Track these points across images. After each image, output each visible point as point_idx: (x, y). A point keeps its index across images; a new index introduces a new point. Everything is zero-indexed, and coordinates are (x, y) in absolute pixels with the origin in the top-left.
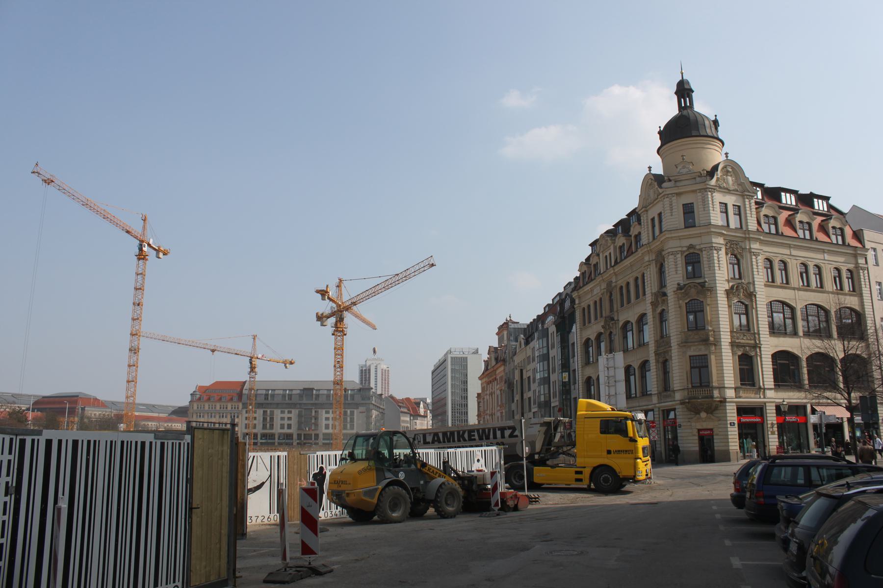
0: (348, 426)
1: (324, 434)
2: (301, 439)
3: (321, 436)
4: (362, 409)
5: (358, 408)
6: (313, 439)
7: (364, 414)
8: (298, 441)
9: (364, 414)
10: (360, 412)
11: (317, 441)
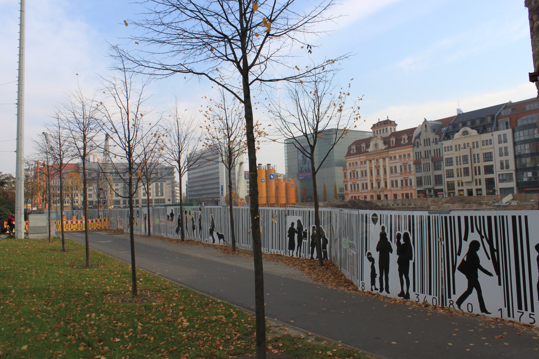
0: (160, 194)
1: (142, 200)
2: (126, 204)
3: (140, 202)
4: (168, 182)
5: (165, 182)
6: (135, 203)
7: (170, 185)
8: (124, 205)
9: (171, 185)
10: (168, 184)
11: (138, 205)
